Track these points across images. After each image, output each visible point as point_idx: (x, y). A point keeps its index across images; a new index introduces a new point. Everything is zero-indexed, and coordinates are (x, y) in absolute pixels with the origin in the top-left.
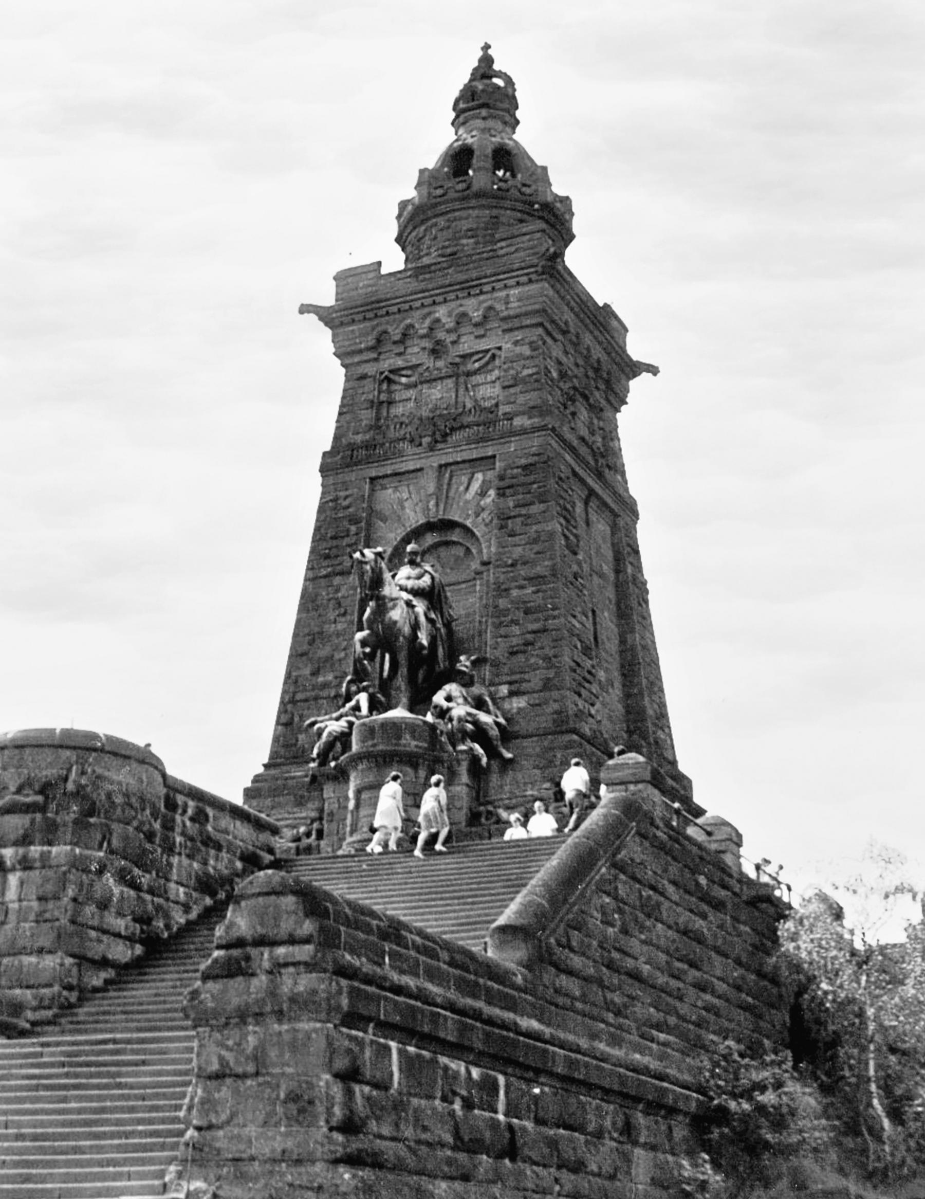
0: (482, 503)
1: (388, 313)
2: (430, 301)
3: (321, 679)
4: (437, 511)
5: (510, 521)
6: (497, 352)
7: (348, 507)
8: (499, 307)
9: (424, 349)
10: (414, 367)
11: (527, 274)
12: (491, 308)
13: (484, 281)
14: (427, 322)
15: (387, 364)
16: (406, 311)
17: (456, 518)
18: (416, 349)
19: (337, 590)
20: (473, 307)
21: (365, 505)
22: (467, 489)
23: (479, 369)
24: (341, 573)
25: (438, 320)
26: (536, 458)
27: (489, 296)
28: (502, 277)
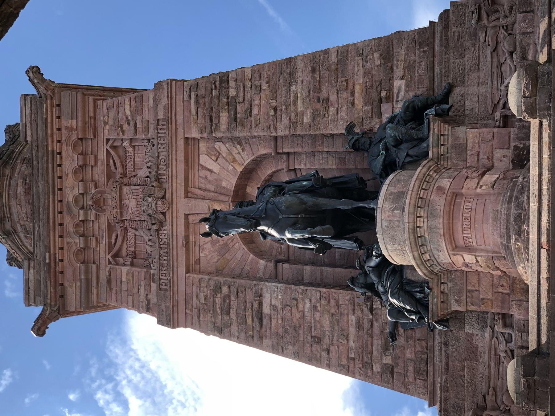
0: (224, 155)
1: (62, 249)
2: (58, 205)
3: (352, 330)
4: (224, 202)
5: (239, 116)
6: (110, 143)
7: (206, 297)
8: (74, 137)
9: (97, 217)
10: (110, 229)
11: (52, 106)
12: (74, 147)
13: (50, 149)
14: (75, 210)
15: (104, 255)
16: (63, 231)
18: (96, 225)
21: (206, 277)
22: (211, 171)
23: (123, 165)
24: (260, 304)
25: (76, 200)
26: (193, 94)
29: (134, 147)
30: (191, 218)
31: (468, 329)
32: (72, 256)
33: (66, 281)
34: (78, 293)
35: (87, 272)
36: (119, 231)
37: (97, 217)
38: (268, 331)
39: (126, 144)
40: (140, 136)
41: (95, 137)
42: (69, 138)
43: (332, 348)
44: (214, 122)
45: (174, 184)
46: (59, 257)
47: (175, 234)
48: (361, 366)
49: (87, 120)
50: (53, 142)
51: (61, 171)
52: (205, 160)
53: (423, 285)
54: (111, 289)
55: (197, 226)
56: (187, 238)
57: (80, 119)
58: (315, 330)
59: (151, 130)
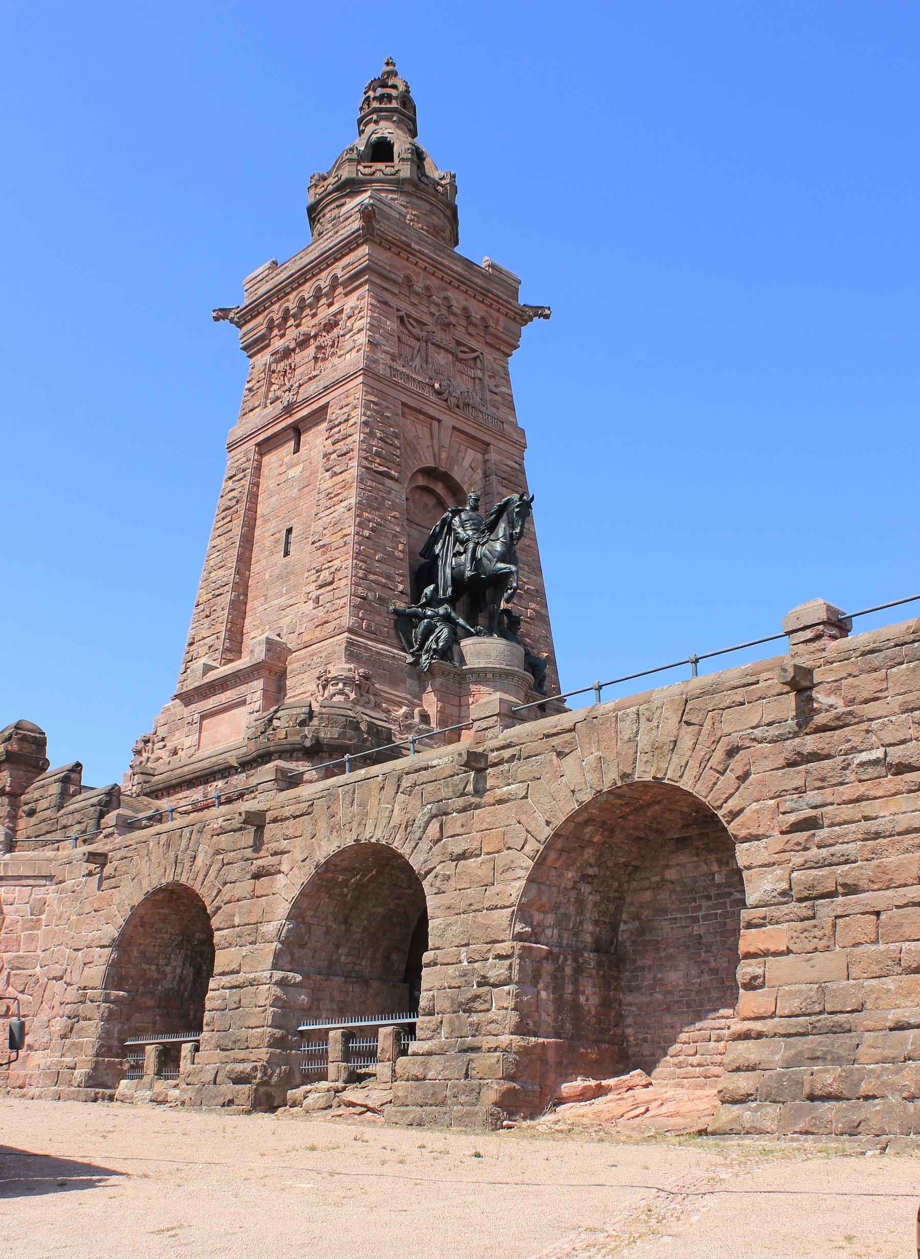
1: (416, 264)
8: (492, 324)
9: (432, 315)
10: (421, 324)
13: (490, 295)
14: (442, 294)
15: (406, 307)
16: (429, 273)
17: (457, 478)
19: (389, 493)
20: (477, 310)
22: (464, 458)
24: (391, 478)
25: (446, 299)
26: (517, 467)
27: (486, 308)
28: (501, 301)
29: (474, 379)
30: (436, 423)
31: (409, 681)
32: (407, 272)
33: (392, 255)
34: (380, 263)
35: (395, 282)
36: (417, 331)
37: (432, 315)
38: (373, 478)
39: (479, 374)
40: (489, 396)
41: (487, 343)
42: (492, 317)
43: (371, 542)
44: (504, 481)
45: (462, 419)
46: (412, 258)
47: (429, 403)
48: (363, 567)
49: (499, 342)
50: (493, 300)
51: (470, 296)
52: (471, 455)
53: (451, 660)
54: (379, 301)
55: (428, 426)
56: (424, 414)
57: (500, 335)
58: (381, 530)
59: (494, 410)
